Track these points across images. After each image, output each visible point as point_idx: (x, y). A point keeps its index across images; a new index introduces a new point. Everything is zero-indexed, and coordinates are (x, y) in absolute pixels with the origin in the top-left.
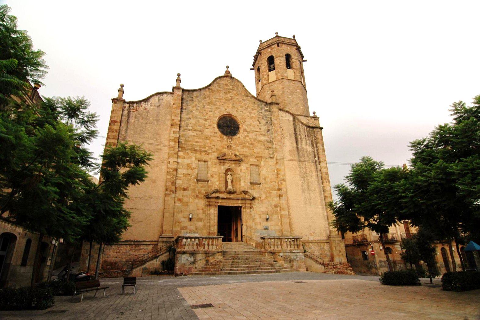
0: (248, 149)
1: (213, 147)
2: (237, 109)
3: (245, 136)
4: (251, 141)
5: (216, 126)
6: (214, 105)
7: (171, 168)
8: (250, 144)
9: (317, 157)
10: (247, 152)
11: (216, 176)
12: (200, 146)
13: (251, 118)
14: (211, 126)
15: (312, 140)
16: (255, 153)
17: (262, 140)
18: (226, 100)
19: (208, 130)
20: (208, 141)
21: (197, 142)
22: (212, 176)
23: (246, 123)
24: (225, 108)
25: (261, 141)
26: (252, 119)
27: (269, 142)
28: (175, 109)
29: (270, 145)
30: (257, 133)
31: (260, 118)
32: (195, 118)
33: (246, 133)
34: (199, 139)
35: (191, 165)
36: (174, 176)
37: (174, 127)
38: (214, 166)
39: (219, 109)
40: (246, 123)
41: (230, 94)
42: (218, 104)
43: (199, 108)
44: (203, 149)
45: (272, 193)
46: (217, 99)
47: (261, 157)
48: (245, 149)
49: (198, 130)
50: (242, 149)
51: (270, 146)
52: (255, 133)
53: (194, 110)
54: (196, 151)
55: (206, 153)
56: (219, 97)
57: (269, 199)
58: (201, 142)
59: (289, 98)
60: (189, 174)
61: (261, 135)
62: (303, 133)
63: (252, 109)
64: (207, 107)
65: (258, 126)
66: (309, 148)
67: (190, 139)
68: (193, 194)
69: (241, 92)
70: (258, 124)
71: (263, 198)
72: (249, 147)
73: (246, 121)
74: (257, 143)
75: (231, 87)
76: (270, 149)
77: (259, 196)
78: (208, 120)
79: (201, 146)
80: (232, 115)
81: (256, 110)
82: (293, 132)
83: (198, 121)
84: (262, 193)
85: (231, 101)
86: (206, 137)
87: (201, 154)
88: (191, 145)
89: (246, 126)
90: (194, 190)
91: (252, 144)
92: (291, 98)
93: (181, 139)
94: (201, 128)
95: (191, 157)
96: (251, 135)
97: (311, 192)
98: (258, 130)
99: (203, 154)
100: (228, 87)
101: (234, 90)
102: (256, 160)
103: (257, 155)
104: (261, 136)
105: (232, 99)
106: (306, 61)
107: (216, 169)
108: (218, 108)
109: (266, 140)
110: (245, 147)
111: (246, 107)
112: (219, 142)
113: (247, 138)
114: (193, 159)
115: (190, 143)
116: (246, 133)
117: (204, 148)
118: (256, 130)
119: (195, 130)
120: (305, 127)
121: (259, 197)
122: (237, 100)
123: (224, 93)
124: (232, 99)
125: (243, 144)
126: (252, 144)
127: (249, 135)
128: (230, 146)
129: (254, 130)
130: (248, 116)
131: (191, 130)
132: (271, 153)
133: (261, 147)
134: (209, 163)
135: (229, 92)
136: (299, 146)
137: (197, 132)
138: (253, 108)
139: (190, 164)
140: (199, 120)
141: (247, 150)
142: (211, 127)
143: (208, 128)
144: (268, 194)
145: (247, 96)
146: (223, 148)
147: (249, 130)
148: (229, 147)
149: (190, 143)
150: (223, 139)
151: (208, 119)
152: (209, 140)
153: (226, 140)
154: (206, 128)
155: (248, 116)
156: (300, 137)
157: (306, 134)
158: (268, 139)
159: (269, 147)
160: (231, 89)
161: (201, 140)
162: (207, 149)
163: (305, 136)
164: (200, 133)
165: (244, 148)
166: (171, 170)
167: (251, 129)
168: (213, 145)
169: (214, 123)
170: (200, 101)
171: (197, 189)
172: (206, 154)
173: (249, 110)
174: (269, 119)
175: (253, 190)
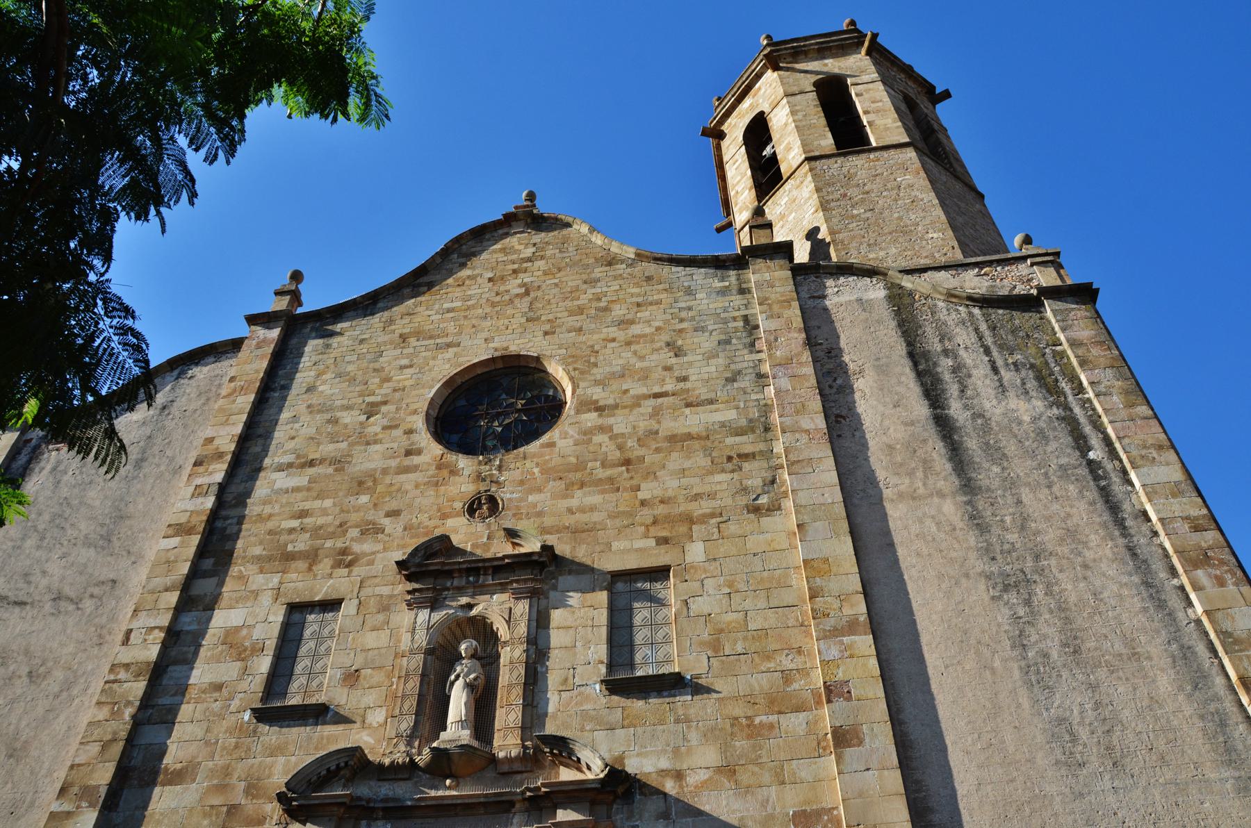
0: (603, 492)
1: (386, 522)
2: (547, 327)
3: (588, 433)
4: (620, 448)
5: (419, 422)
6: (431, 337)
7: (127, 666)
8: (614, 465)
9: (1095, 440)
10: (592, 509)
11: (378, 677)
12: (316, 532)
13: (628, 344)
14: (396, 427)
15: (1038, 362)
16: (643, 503)
17: (694, 431)
18: (493, 305)
19: (377, 447)
20: (364, 499)
21: (303, 514)
22: (352, 678)
23: (598, 373)
24: (485, 335)
25: (689, 437)
26: (633, 347)
27: (740, 432)
28: (232, 398)
29: (747, 443)
30: (660, 400)
31: (681, 331)
32: (319, 412)
33: (591, 418)
34: (317, 498)
35: (244, 632)
36: (129, 703)
37: (201, 469)
38: (381, 617)
39: (452, 350)
40: (595, 371)
41: (521, 275)
42: (451, 327)
43: (350, 368)
44: (329, 544)
45: (771, 726)
46: (449, 310)
47: (690, 520)
48: (579, 498)
49: (322, 461)
50: (565, 497)
51: (748, 449)
52: (652, 402)
53: (324, 382)
54: (289, 557)
55: (345, 560)
56: (458, 304)
57: (744, 777)
58: (324, 512)
59: (853, 216)
60: (218, 687)
61: (688, 405)
62: (963, 337)
63: (639, 305)
64: (390, 354)
65: (667, 369)
66: (1029, 408)
67: (268, 510)
68: (216, 800)
69: (577, 258)
70: (674, 360)
71: (703, 775)
72: (611, 480)
73: (596, 365)
74: (658, 450)
75: (529, 252)
76: (746, 466)
77: (664, 764)
78: (384, 409)
79: (321, 527)
80: (519, 356)
81: (659, 302)
82: (901, 349)
83: (334, 421)
84: (694, 737)
85: (523, 304)
86: (360, 483)
87: (310, 569)
88: (270, 532)
89: (597, 383)
90: (226, 771)
91: (627, 462)
92: (869, 214)
93: (226, 518)
94: (344, 445)
95: (256, 594)
96: (620, 423)
97: (1102, 673)
98: (669, 387)
99: (325, 565)
100: (515, 257)
101: (542, 258)
102: (652, 542)
103: (661, 510)
104: (687, 411)
105: (527, 293)
106: (946, 95)
107: (384, 636)
108: (449, 345)
109: (723, 425)
110: (582, 485)
111: (603, 304)
112: (435, 494)
113: (599, 438)
114: (266, 599)
115: (270, 525)
116: (595, 414)
117: (332, 536)
118: (657, 389)
119: (311, 463)
120: (976, 311)
121: (663, 773)
122: (556, 291)
123: (490, 280)
124: (527, 293)
125: (574, 476)
126: (627, 462)
127: (611, 421)
128: (492, 500)
129: (644, 390)
130: (614, 340)
131: (290, 465)
132: (755, 482)
133: (687, 464)
134: (348, 608)
135: (515, 271)
136: (955, 409)
137: (311, 471)
138: (640, 300)
139: (237, 629)
140: (339, 414)
141: (596, 499)
142: (397, 433)
143: (375, 442)
144: (741, 744)
145: (610, 264)
146: (444, 517)
147: (611, 402)
148: (483, 505)
149: (270, 525)
150: (454, 472)
151: (385, 403)
152: (371, 491)
153: (466, 473)
154: (368, 443)
155: (614, 340)
156: (946, 363)
157: (989, 341)
158: (731, 415)
159: (744, 457)
160: (529, 260)
161: (328, 503)
162: (352, 539)
163: (987, 351)
164: (330, 470)
165: (579, 493)
166: (122, 675)
167: (626, 391)
168: (388, 515)
169: (415, 412)
170: (362, 341)
171: (240, 769)
172: (338, 564)
173: (619, 311)
174: (741, 324)
175: (620, 732)
